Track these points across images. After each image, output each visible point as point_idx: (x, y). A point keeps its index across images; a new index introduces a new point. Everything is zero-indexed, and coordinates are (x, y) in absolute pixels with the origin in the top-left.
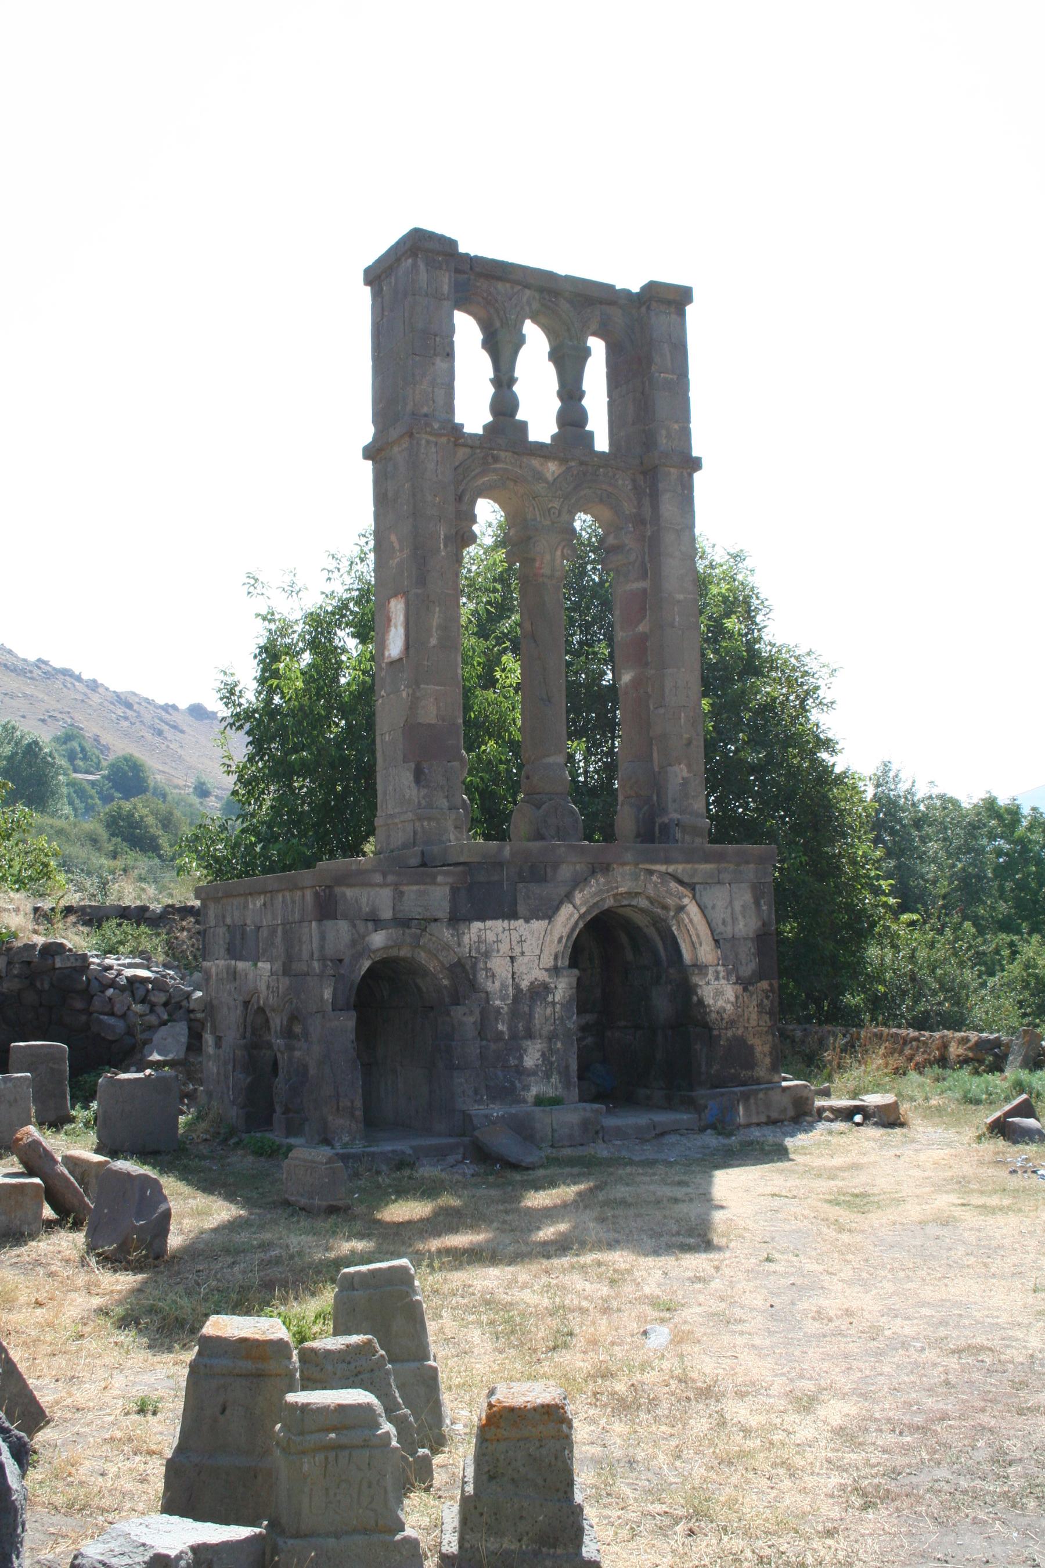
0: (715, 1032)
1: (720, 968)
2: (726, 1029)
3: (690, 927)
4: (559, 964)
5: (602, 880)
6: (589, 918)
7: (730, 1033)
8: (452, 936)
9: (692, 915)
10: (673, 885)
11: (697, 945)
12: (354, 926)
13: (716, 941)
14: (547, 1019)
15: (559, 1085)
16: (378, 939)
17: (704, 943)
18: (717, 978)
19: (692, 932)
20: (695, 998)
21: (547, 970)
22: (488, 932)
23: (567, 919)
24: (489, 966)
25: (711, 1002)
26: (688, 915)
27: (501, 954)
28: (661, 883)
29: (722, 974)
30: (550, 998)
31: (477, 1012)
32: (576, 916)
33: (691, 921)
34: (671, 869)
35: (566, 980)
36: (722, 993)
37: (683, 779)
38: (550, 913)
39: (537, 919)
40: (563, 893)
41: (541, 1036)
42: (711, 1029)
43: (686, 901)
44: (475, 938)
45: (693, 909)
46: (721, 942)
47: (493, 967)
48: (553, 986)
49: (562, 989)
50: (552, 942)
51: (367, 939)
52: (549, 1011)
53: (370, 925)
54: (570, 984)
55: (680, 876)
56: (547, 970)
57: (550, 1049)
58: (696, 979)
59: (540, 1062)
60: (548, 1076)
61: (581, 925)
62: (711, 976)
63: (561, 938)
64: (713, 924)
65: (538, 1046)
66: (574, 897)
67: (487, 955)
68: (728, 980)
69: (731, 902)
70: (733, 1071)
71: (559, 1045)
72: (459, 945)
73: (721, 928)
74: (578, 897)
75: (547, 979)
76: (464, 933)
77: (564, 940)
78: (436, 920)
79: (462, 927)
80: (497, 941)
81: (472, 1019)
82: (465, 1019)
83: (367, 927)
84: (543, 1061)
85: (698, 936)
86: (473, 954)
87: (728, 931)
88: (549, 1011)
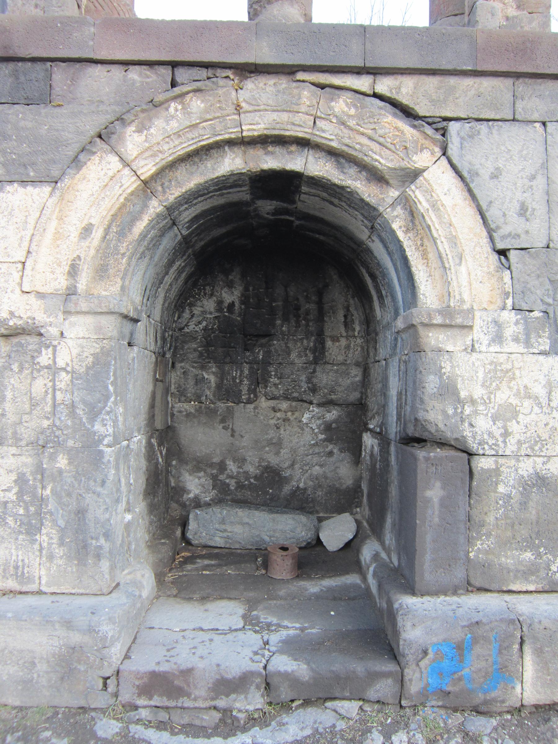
0: (483, 464)
1: (509, 316)
2: (517, 457)
3: (432, 218)
4: (82, 285)
5: (197, 104)
6: (174, 194)
7: (526, 468)
9: (439, 191)
10: (391, 121)
11: (451, 262)
13: (503, 253)
14: (34, 404)
15: (59, 552)
17: (468, 257)
18: (498, 338)
19: (438, 231)
20: (431, 383)
21: (40, 295)
23: (101, 188)
25: (478, 392)
26: (429, 192)
28: (359, 117)
29: (509, 332)
30: (45, 358)
32: (130, 183)
33: (434, 206)
34: (384, 85)
35: (89, 320)
36: (508, 375)
37: (507, 18)
38: (55, 173)
39: (23, 183)
40: (91, 126)
41: (17, 439)
42: (470, 454)
43: (421, 160)
45: (439, 178)
46: (512, 255)
48: (54, 331)
49: (76, 340)
50: (58, 236)
52: (40, 385)
54: (99, 329)
55: (405, 100)
56: (40, 295)
57: (40, 470)
58: (433, 339)
59: (12, 496)
60: (31, 528)
61: (155, 207)
62: (480, 333)
63: (87, 230)
64: (493, 214)
65: (11, 462)
66: (121, 139)
68: (528, 343)
69: (545, 166)
70: (528, 555)
71: (62, 462)
73: (510, 226)
74: (133, 141)
75: (41, 317)
77: (98, 234)
84: (20, 494)
85: (453, 241)
87: (535, 233)
88: (40, 385)
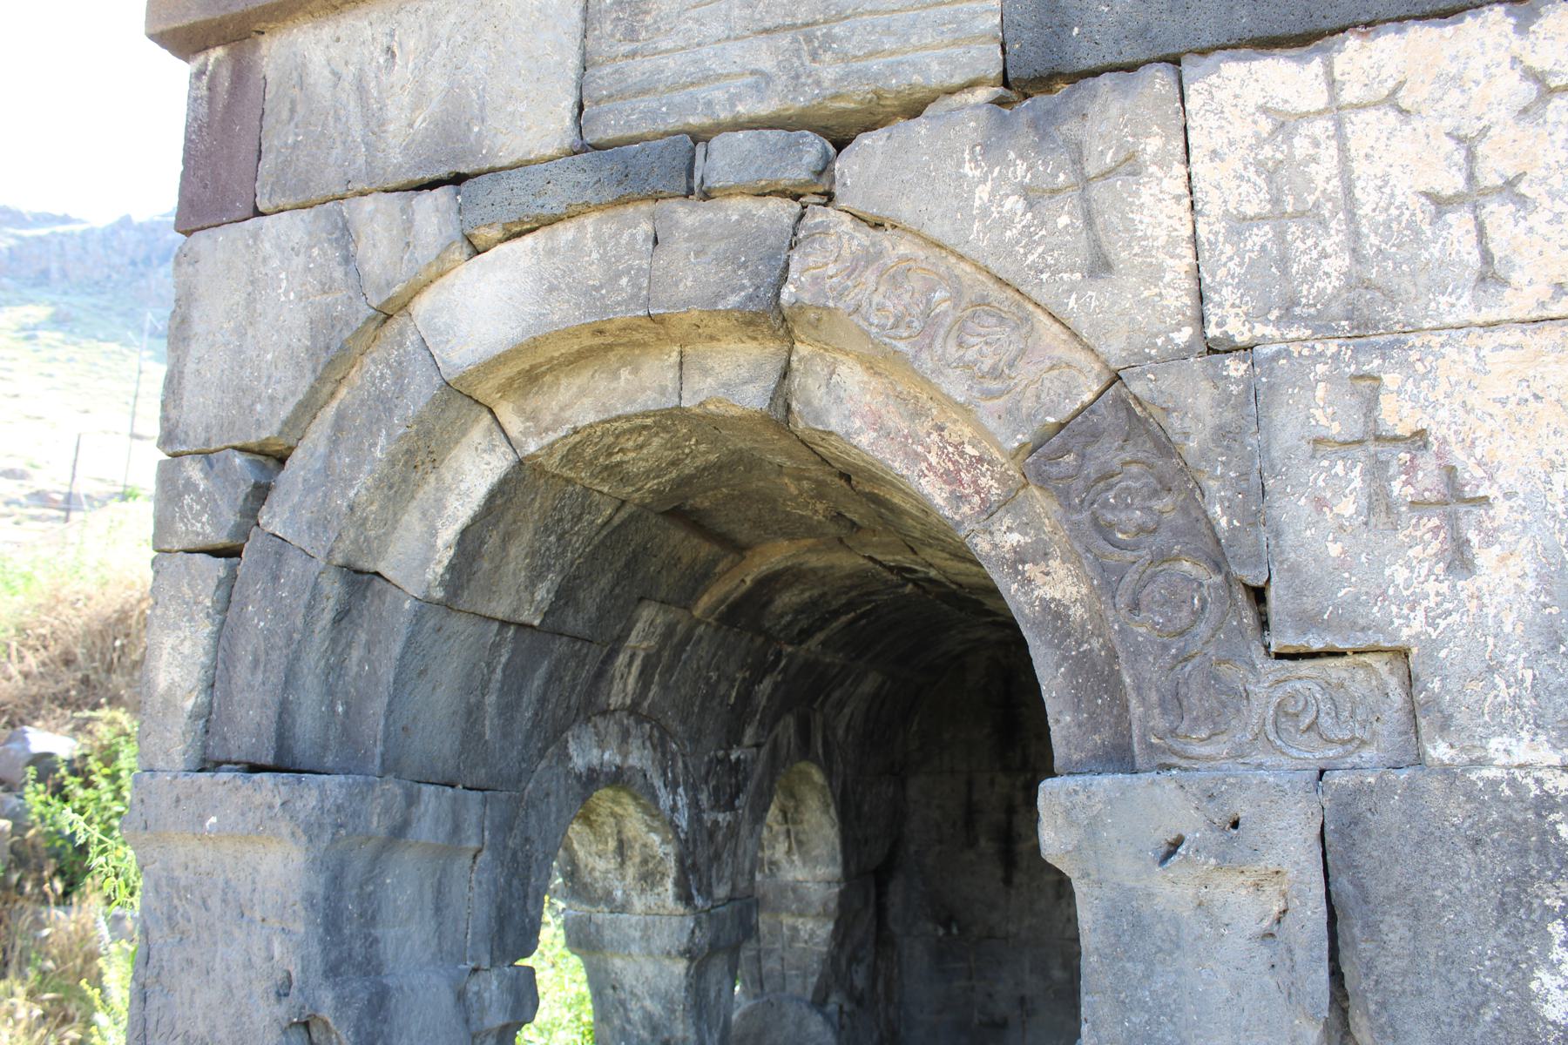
8: (1033, 196)
12: (344, 235)
16: (485, 304)
22: (1366, 129)
24: (1397, 414)
27: (1519, 302)
31: (1290, 844)
44: (1228, 186)
47: (1439, 425)
51: (422, 306)
53: (432, 208)
67: (1366, 322)
72: (1100, 266)
76: (1130, 165)
78: (914, 109)
79: (1113, 117)
80: (1473, 196)
81: (1244, 904)
82: (1172, 890)
83: (409, 225)
86: (1230, 323)
